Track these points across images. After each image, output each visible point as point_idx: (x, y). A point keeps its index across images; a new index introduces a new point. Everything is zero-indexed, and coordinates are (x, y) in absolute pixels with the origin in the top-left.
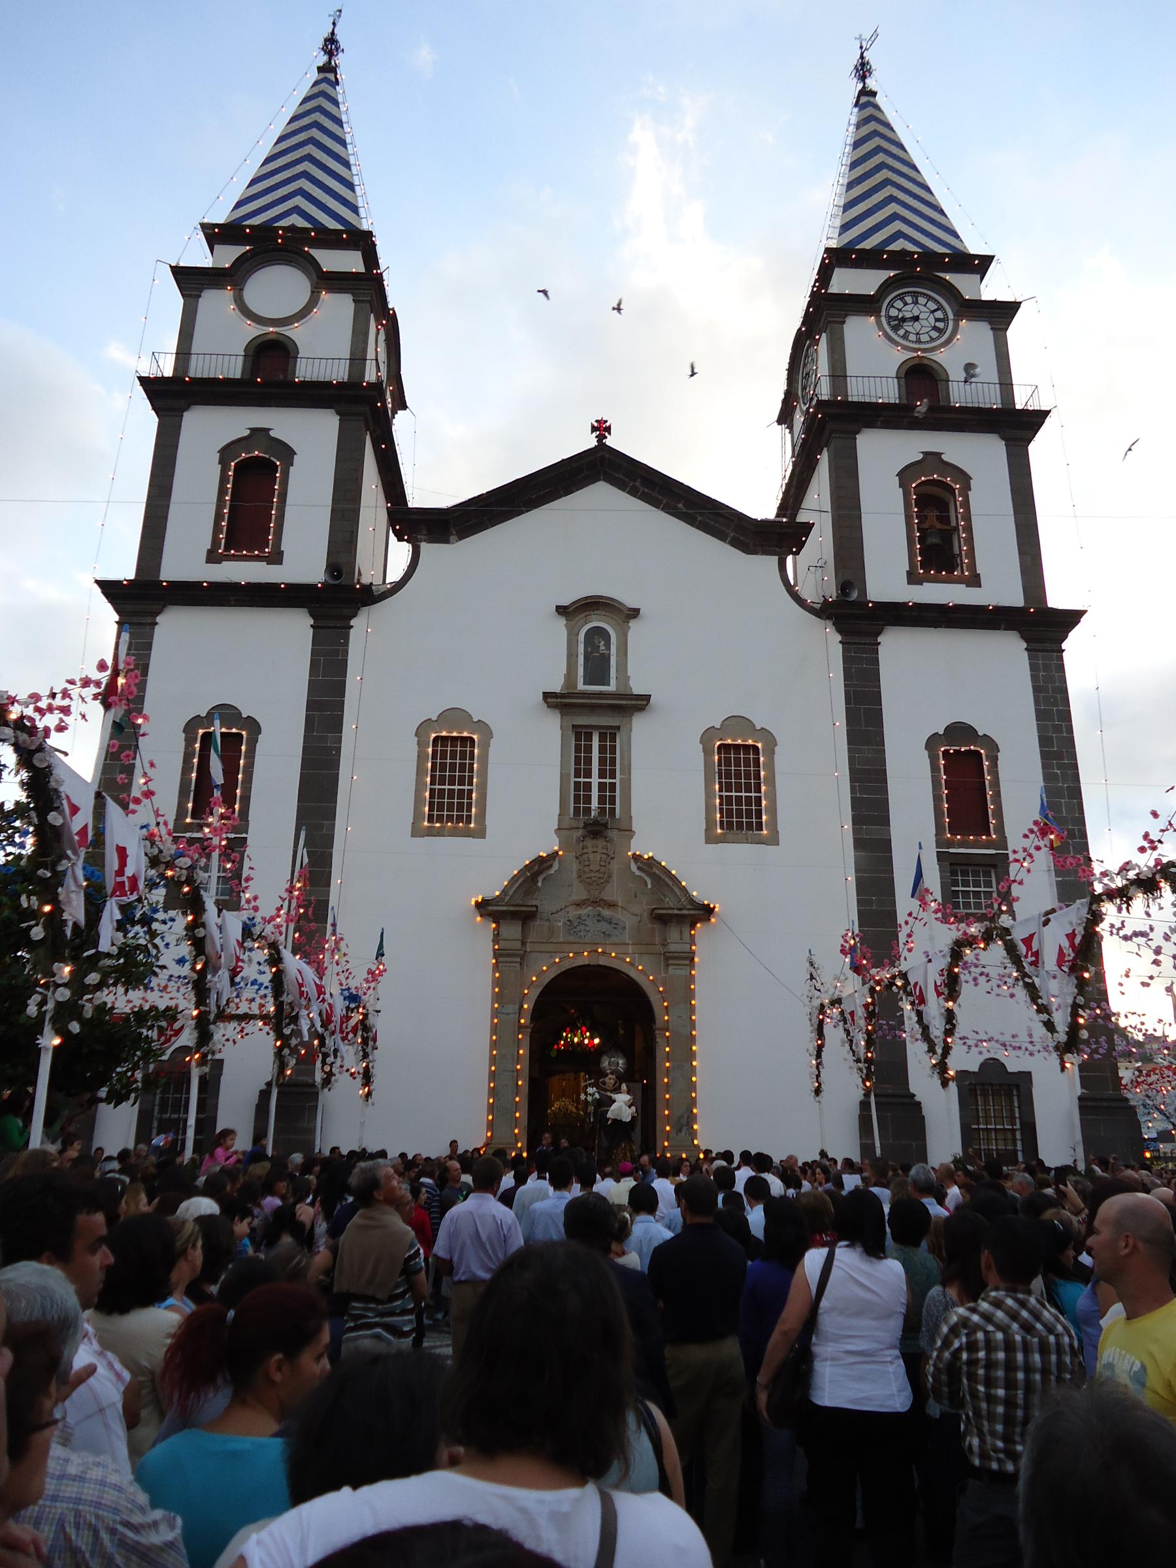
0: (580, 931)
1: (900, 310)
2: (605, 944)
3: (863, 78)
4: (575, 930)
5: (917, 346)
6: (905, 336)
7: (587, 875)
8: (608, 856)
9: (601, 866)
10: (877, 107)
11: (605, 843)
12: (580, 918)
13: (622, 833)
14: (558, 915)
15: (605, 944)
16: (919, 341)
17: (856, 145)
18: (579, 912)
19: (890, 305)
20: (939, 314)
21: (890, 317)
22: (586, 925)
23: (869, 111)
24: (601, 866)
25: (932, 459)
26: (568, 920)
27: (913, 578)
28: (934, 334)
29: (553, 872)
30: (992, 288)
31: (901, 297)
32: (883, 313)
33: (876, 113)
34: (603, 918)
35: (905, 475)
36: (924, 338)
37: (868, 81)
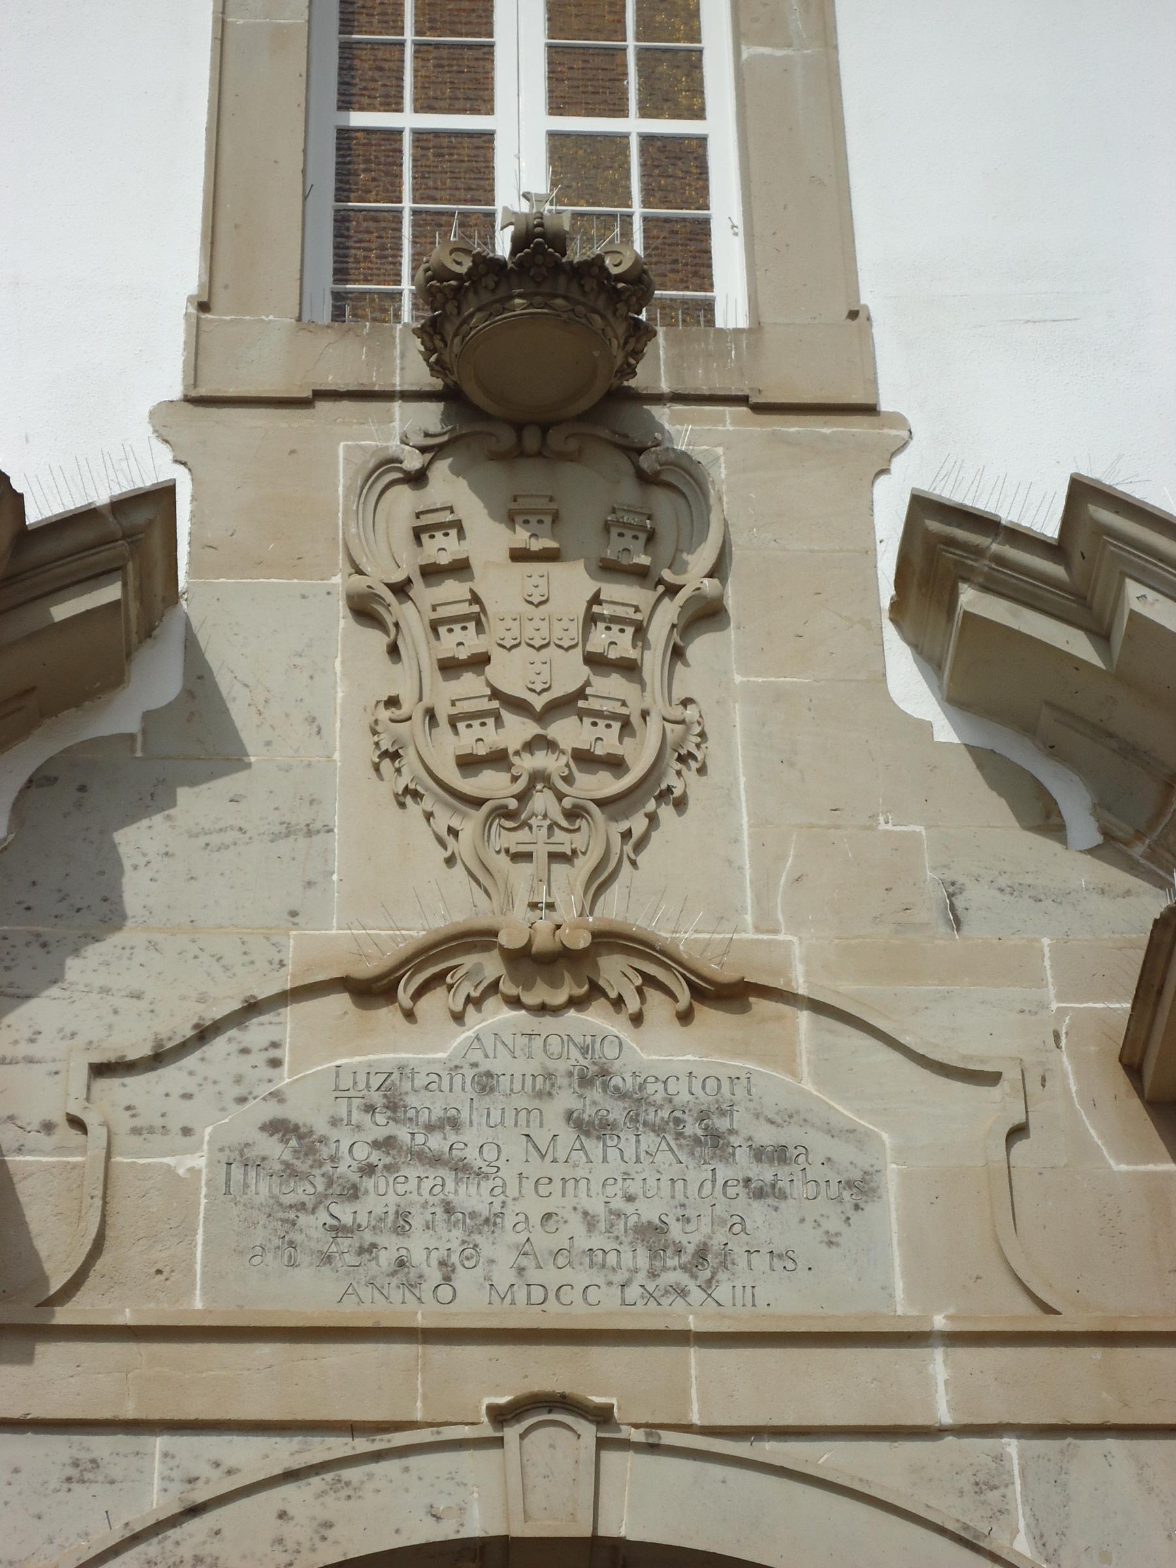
0: (401, 1223)
2: (682, 1338)
4: (345, 1213)
7: (470, 740)
8: (672, 590)
9: (595, 661)
11: (628, 492)
12: (394, 1106)
13: (794, 427)
14: (172, 1076)
15: (682, 1338)
18: (388, 1058)
22: (461, 1168)
24: (595, 661)
26: (278, 1128)
29: (130, 723)
34: (636, 1099)
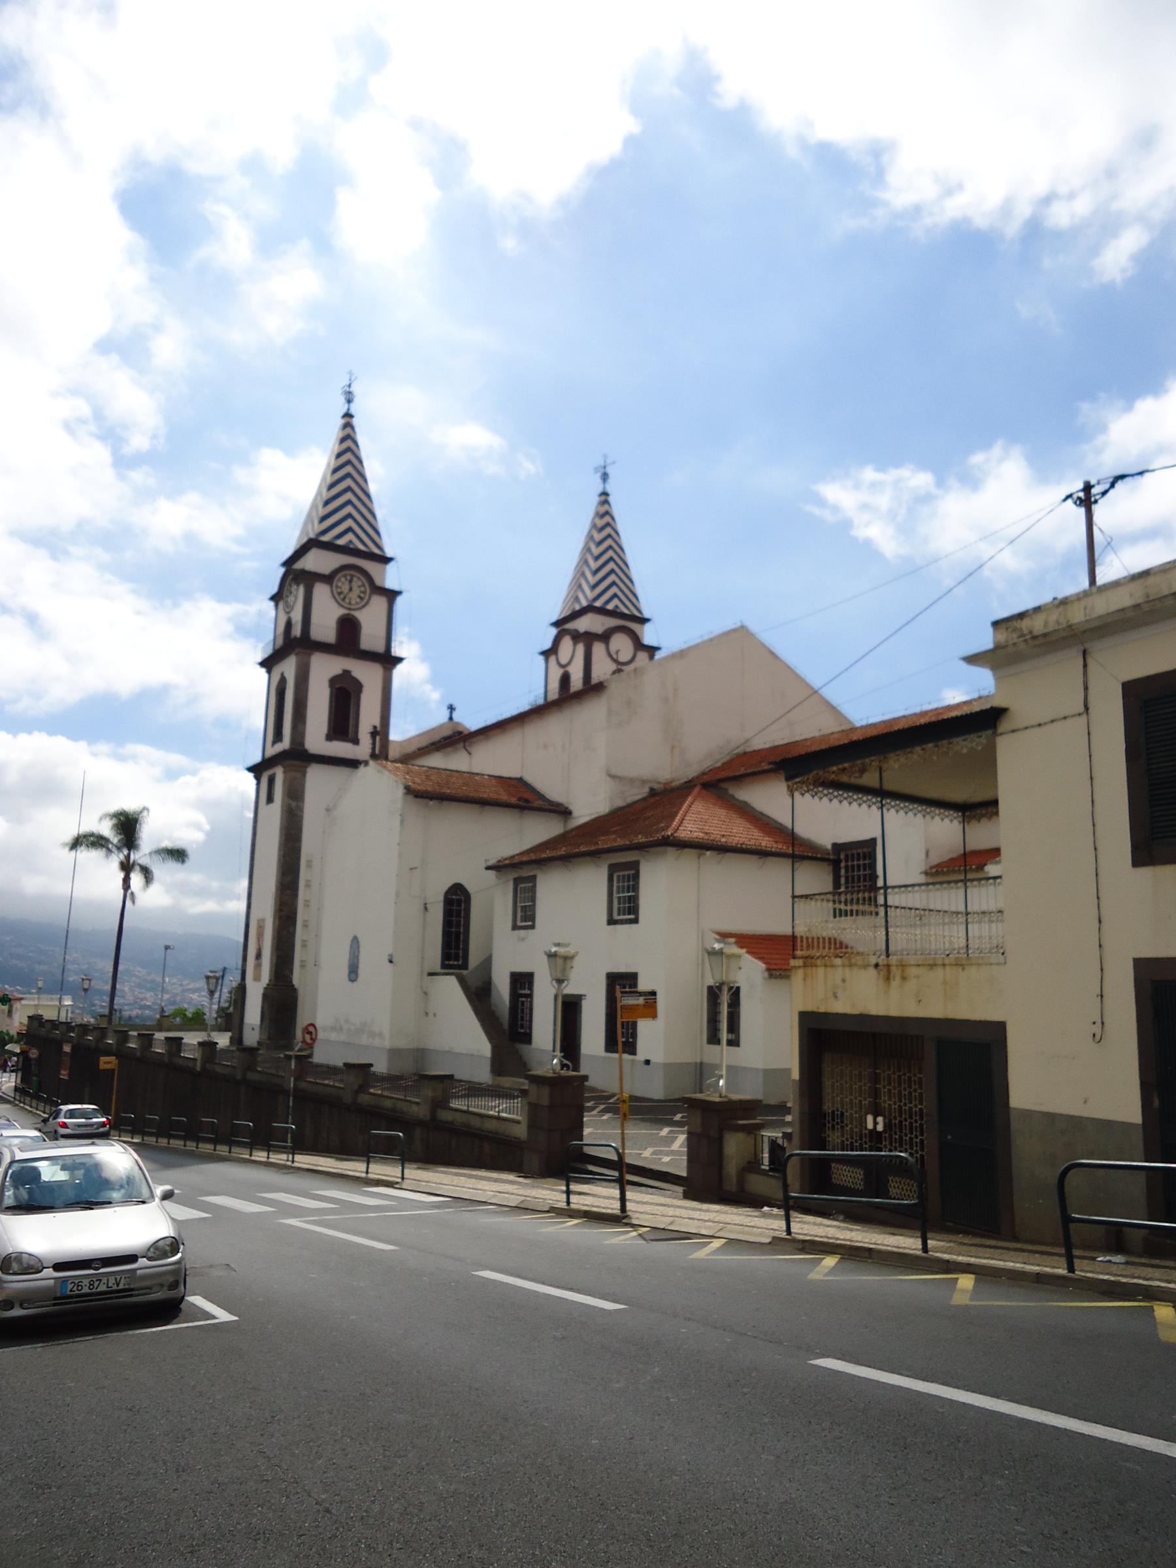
1: (343, 583)
3: (349, 401)
5: (348, 606)
6: (344, 599)
10: (353, 428)
16: (350, 603)
17: (339, 456)
19: (339, 580)
20: (362, 589)
21: (337, 587)
23: (348, 430)
25: (346, 673)
27: (330, 737)
28: (358, 600)
30: (390, 583)
31: (345, 576)
32: (334, 584)
33: (352, 435)
35: (333, 681)
36: (353, 602)
37: (352, 405)
